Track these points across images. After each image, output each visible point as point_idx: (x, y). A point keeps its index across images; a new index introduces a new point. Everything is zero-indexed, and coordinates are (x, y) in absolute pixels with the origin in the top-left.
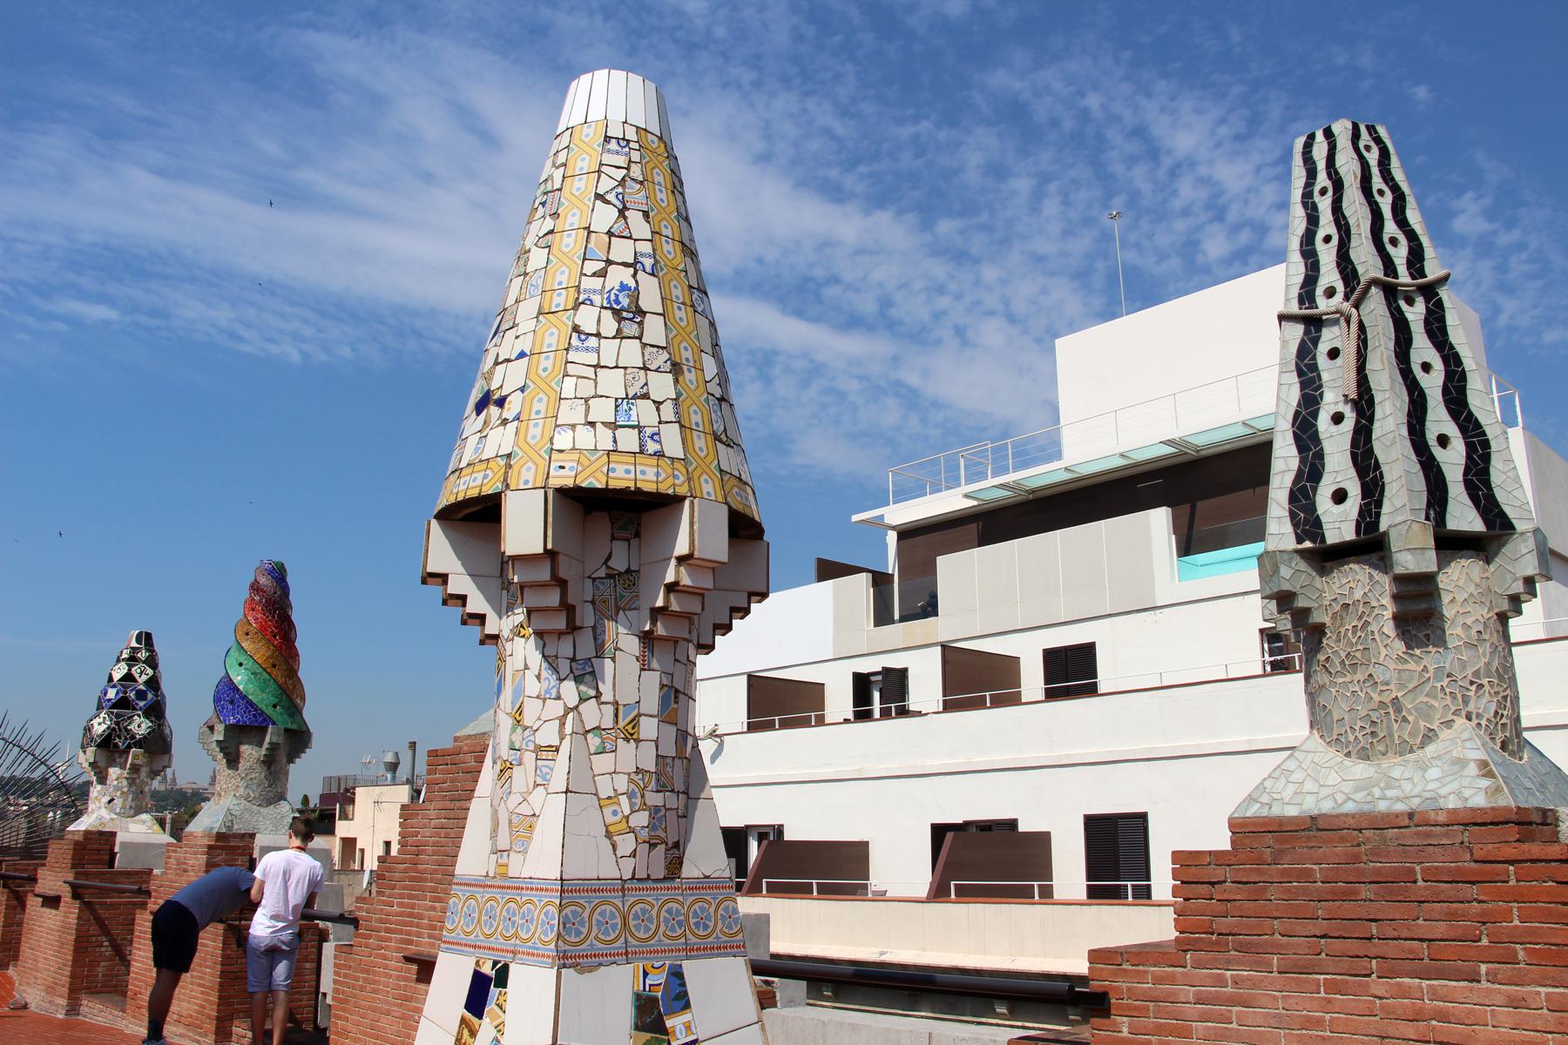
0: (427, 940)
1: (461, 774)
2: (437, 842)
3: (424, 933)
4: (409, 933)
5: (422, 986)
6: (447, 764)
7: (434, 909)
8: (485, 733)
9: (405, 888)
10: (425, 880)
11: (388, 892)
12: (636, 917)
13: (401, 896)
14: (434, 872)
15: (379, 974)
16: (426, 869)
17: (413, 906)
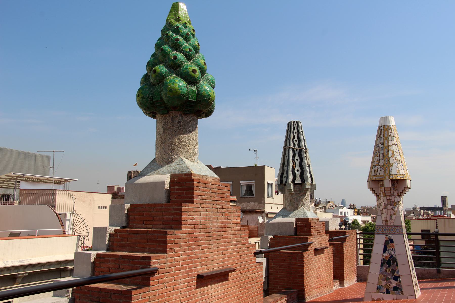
0: (200, 267)
1: (211, 193)
2: (205, 222)
3: (199, 264)
4: (191, 267)
5: (392, 244)
6: (204, 187)
7: (203, 252)
8: (207, 176)
9: (187, 246)
10: (198, 240)
11: (176, 249)
12: (381, 230)
13: (185, 250)
14: (203, 236)
15: (172, 294)
16: (199, 235)
17: (192, 254)
